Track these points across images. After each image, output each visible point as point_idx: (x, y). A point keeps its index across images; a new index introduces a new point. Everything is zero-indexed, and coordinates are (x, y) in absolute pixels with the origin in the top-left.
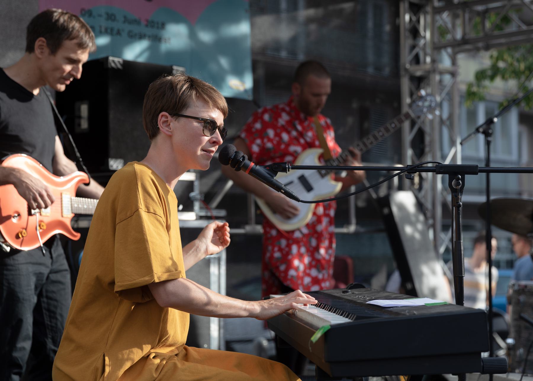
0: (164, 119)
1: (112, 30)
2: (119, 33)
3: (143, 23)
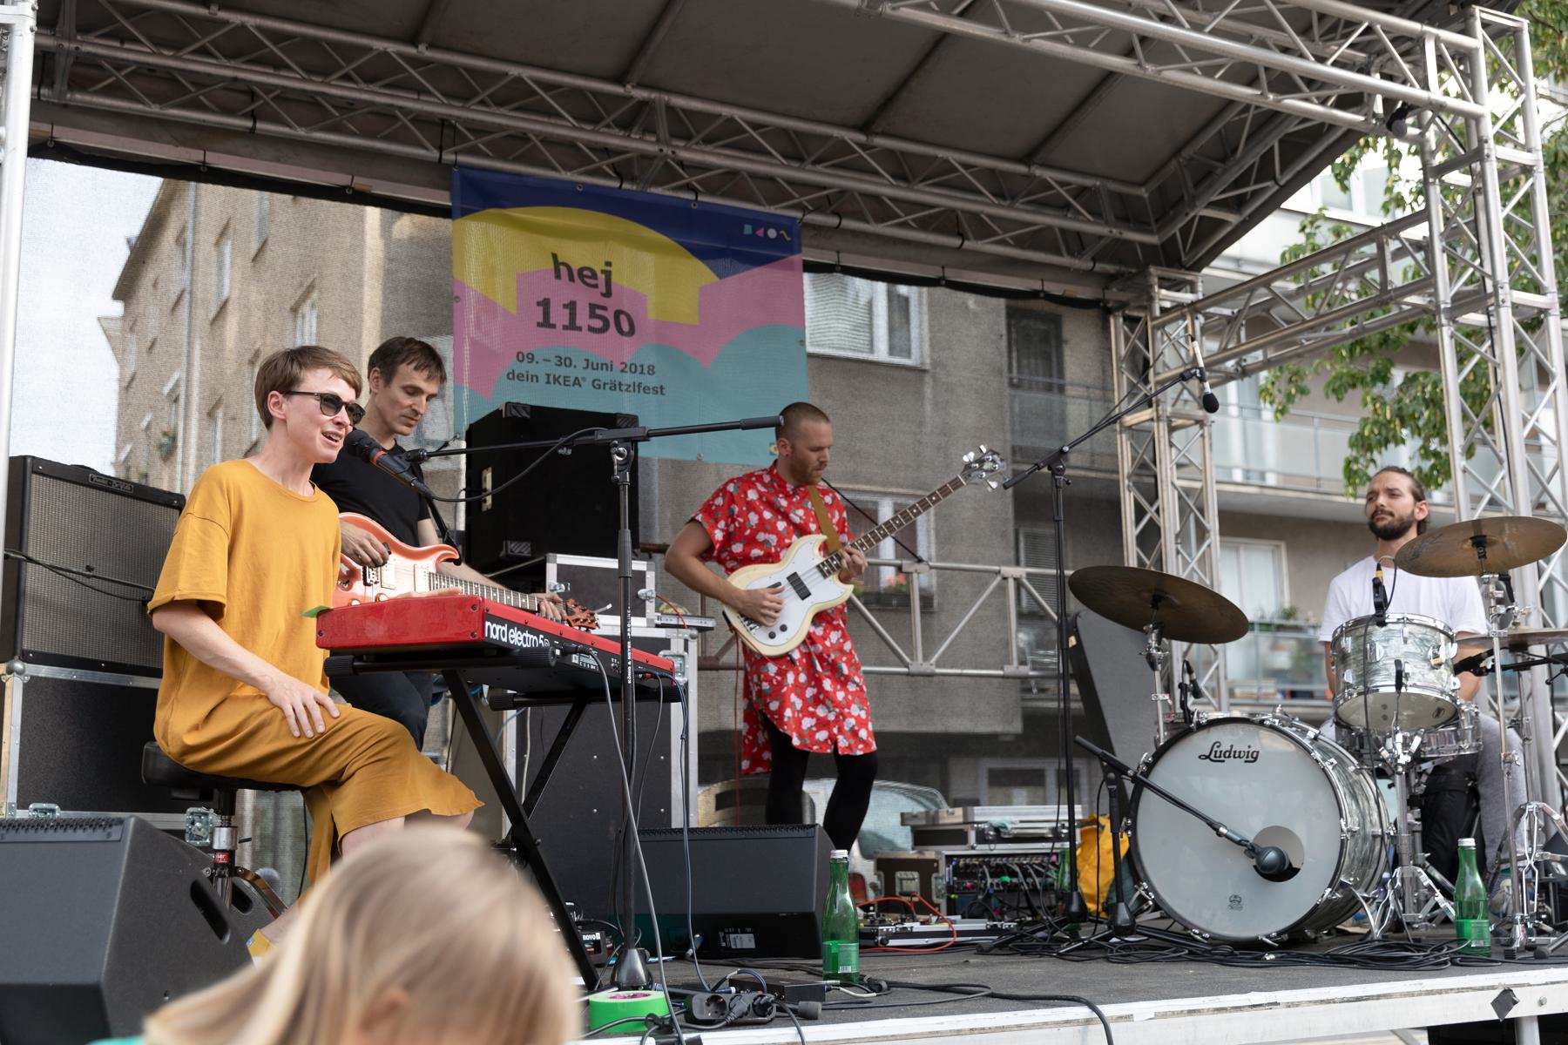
0: (274, 400)
2: (577, 382)
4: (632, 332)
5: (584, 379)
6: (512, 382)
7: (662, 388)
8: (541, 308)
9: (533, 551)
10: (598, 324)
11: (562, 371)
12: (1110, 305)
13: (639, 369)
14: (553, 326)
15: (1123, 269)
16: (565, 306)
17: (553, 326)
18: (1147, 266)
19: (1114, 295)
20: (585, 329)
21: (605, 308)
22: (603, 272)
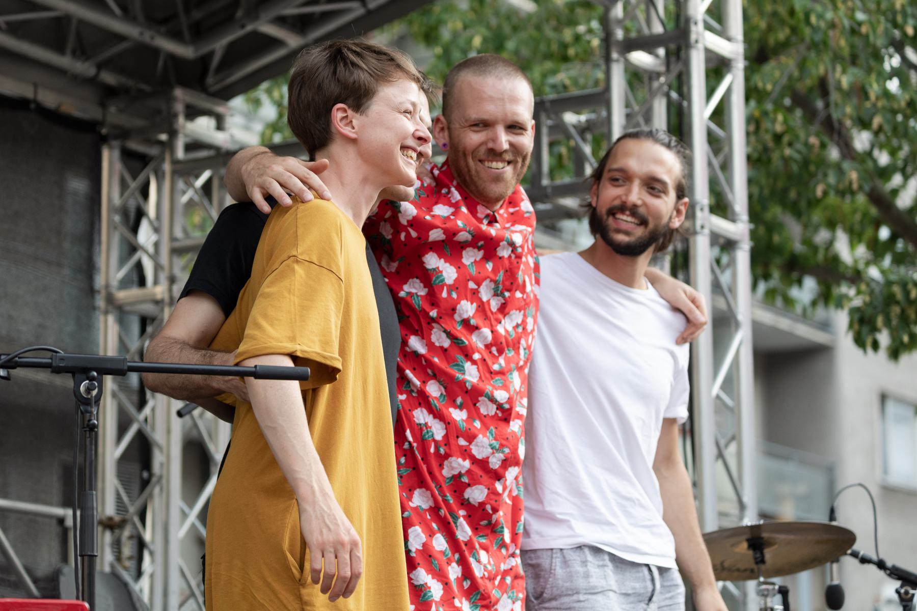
12: (104, 131)
15: (130, 83)
18: (171, 87)
19: (115, 115)
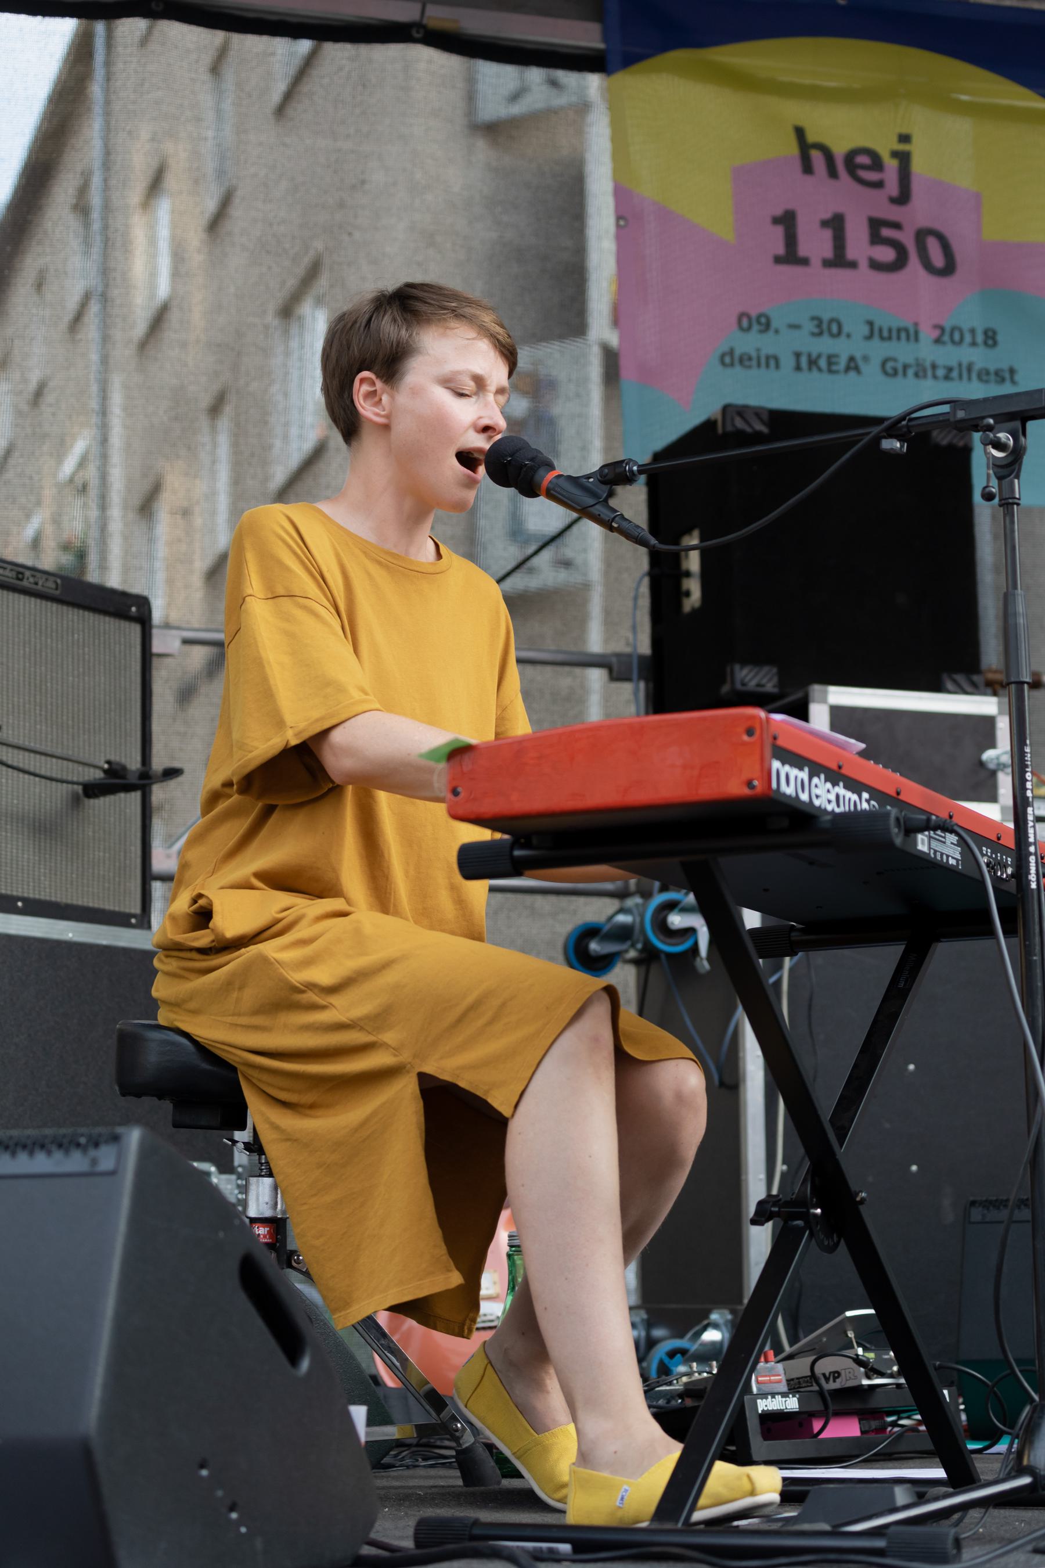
0: (366, 388)
1: (831, 360)
2: (852, 365)
3: (927, 335)
4: (949, 269)
5: (866, 359)
6: (729, 371)
7: (1012, 371)
8: (779, 231)
9: (781, 684)
10: (886, 254)
11: (825, 345)
13: (968, 338)
14: (805, 262)
16: (825, 224)
17: (805, 262)
20: (864, 264)
21: (897, 226)
22: (895, 154)
